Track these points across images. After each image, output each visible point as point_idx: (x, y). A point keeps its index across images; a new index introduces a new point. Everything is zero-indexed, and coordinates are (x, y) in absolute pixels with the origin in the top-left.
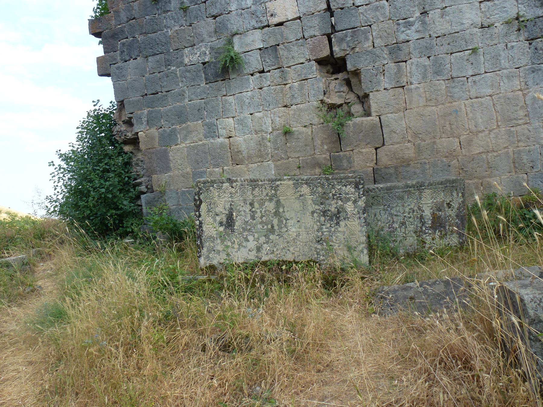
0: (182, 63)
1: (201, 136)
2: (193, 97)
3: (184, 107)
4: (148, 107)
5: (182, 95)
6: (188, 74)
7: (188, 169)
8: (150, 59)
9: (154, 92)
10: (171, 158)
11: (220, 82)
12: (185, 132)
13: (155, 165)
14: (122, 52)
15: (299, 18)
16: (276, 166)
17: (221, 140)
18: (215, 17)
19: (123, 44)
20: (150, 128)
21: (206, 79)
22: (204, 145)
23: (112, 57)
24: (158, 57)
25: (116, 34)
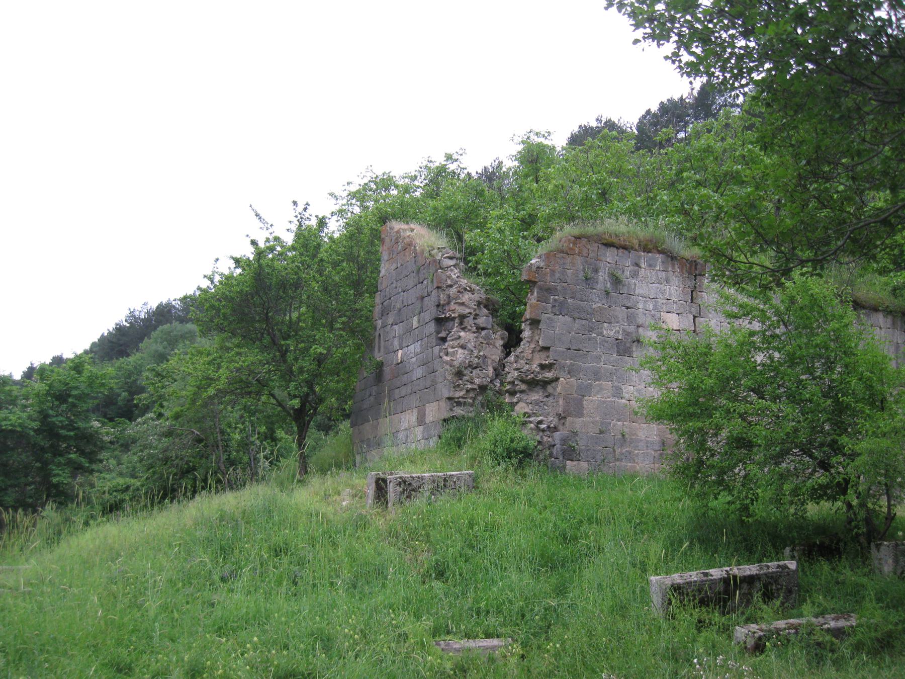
0: (602, 333)
1: (609, 394)
2: (607, 362)
3: (600, 368)
4: (571, 359)
5: (598, 358)
6: (606, 344)
7: (598, 419)
8: (577, 321)
9: (577, 348)
10: (585, 406)
11: (626, 358)
12: (598, 388)
13: (572, 409)
14: (554, 306)
15: (679, 330)
16: (658, 429)
17: (623, 401)
18: (628, 308)
19: (555, 300)
20: (571, 377)
21: (618, 352)
22: (611, 401)
23: (544, 307)
24: (584, 322)
25: (550, 289)
